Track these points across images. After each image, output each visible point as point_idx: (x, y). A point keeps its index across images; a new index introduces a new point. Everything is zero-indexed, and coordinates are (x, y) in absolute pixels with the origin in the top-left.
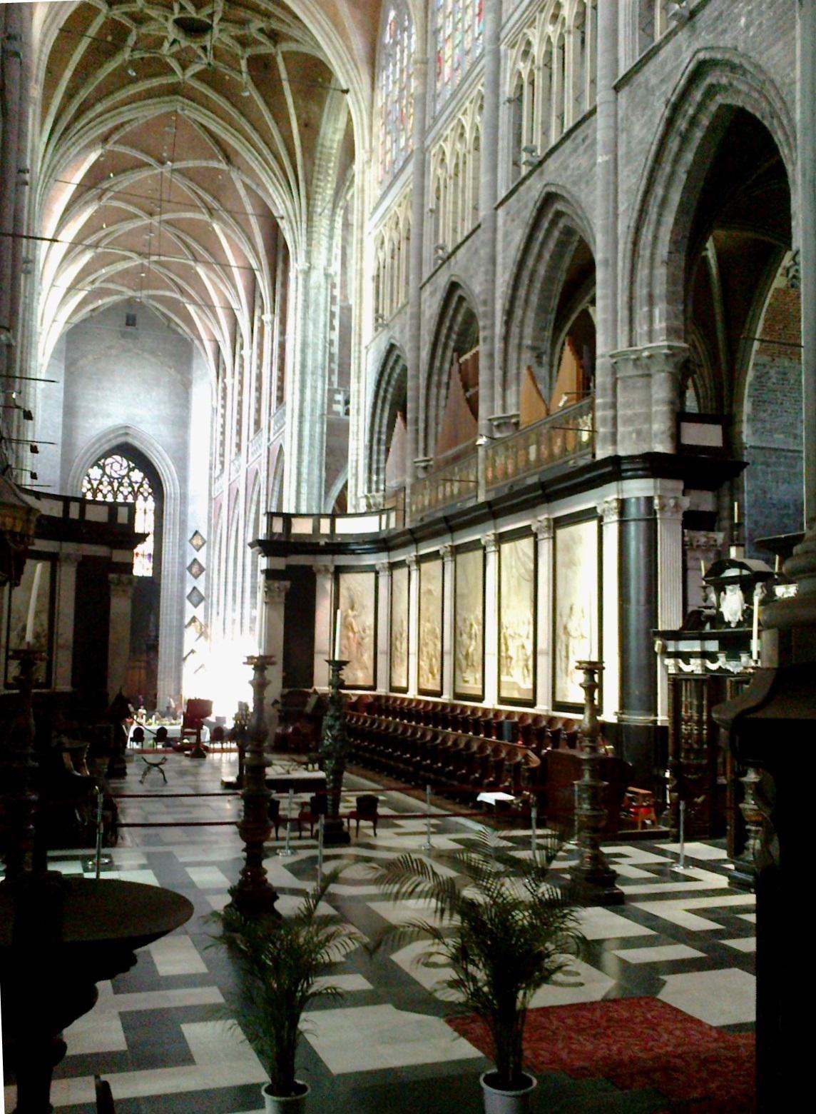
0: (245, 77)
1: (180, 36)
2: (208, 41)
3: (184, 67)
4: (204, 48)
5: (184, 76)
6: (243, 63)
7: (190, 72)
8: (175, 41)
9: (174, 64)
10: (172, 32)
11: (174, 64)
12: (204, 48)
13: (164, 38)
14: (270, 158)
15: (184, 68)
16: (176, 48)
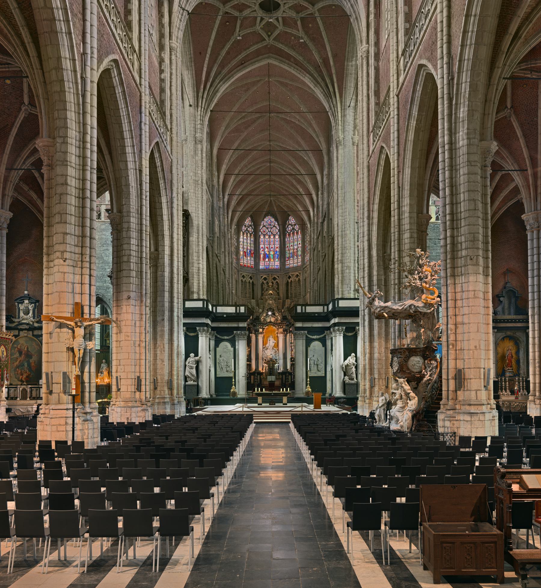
0: (301, 33)
1: (264, 15)
2: (279, 14)
3: (269, 36)
4: (277, 19)
5: (270, 41)
6: (299, 23)
7: (272, 37)
8: (262, 19)
9: (264, 35)
10: (260, 13)
11: (264, 35)
12: (277, 19)
13: (256, 18)
14: (320, 80)
15: (269, 36)
16: (264, 23)
